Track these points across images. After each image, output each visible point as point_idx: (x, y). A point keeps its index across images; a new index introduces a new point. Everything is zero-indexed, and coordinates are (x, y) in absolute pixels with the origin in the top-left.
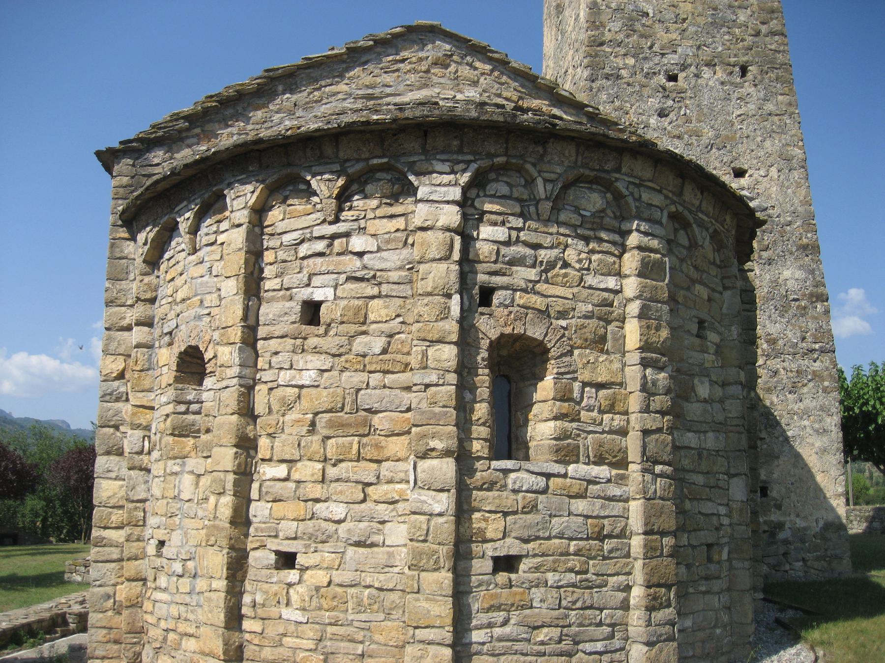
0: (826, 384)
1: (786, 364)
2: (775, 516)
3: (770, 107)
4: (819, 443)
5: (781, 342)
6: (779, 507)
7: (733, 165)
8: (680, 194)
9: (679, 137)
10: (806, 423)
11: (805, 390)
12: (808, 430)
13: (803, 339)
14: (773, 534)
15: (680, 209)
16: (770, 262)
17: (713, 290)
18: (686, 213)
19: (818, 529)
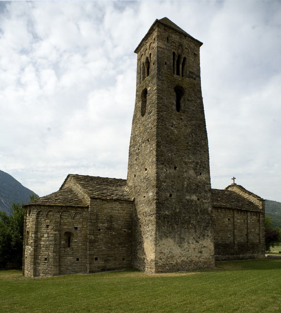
0: (153, 223)
1: (147, 218)
2: (144, 257)
3: (152, 149)
4: (151, 238)
5: (147, 213)
6: (145, 254)
7: (145, 168)
8: (41, 208)
9: (137, 165)
10: (149, 233)
11: (150, 225)
12: (149, 235)
13: (151, 211)
14: (143, 261)
15: (41, 210)
16: (147, 192)
17: (52, 220)
18: (42, 210)
19: (150, 261)
